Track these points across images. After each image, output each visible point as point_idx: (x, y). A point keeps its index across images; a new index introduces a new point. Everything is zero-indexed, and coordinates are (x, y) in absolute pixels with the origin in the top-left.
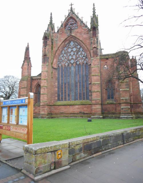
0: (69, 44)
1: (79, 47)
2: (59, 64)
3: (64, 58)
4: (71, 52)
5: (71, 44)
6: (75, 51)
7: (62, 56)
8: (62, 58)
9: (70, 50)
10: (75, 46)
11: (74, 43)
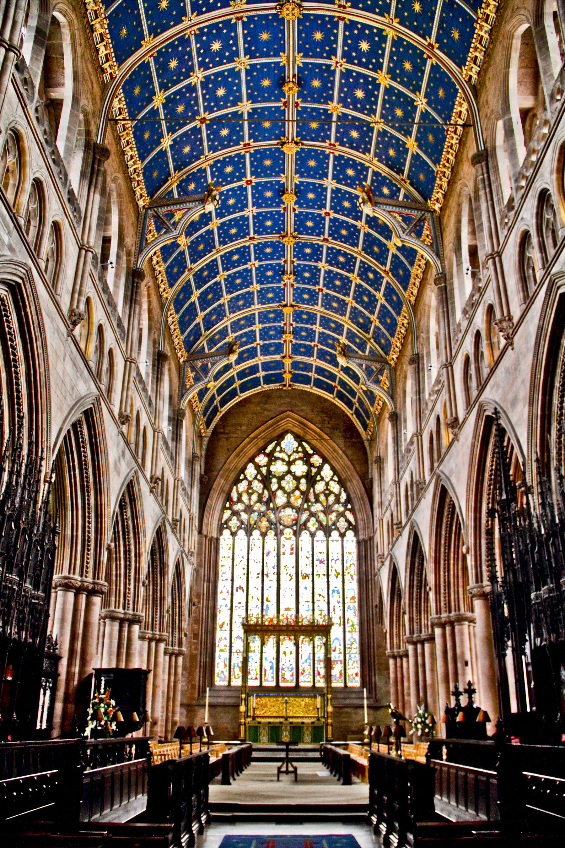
0: (278, 444)
1: (316, 460)
2: (229, 519)
3: (254, 497)
4: (280, 478)
5: (283, 444)
6: (303, 477)
7: (243, 486)
8: (245, 498)
9: (279, 468)
10: (301, 455)
11: (300, 445)
